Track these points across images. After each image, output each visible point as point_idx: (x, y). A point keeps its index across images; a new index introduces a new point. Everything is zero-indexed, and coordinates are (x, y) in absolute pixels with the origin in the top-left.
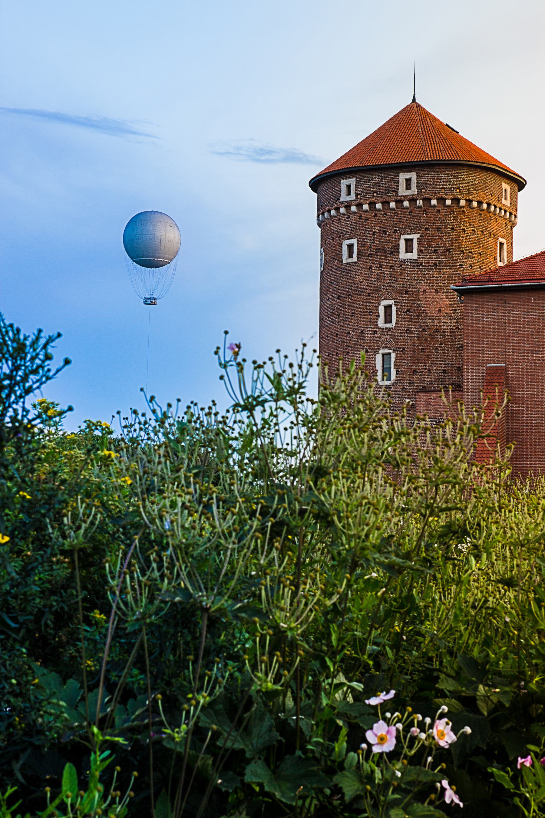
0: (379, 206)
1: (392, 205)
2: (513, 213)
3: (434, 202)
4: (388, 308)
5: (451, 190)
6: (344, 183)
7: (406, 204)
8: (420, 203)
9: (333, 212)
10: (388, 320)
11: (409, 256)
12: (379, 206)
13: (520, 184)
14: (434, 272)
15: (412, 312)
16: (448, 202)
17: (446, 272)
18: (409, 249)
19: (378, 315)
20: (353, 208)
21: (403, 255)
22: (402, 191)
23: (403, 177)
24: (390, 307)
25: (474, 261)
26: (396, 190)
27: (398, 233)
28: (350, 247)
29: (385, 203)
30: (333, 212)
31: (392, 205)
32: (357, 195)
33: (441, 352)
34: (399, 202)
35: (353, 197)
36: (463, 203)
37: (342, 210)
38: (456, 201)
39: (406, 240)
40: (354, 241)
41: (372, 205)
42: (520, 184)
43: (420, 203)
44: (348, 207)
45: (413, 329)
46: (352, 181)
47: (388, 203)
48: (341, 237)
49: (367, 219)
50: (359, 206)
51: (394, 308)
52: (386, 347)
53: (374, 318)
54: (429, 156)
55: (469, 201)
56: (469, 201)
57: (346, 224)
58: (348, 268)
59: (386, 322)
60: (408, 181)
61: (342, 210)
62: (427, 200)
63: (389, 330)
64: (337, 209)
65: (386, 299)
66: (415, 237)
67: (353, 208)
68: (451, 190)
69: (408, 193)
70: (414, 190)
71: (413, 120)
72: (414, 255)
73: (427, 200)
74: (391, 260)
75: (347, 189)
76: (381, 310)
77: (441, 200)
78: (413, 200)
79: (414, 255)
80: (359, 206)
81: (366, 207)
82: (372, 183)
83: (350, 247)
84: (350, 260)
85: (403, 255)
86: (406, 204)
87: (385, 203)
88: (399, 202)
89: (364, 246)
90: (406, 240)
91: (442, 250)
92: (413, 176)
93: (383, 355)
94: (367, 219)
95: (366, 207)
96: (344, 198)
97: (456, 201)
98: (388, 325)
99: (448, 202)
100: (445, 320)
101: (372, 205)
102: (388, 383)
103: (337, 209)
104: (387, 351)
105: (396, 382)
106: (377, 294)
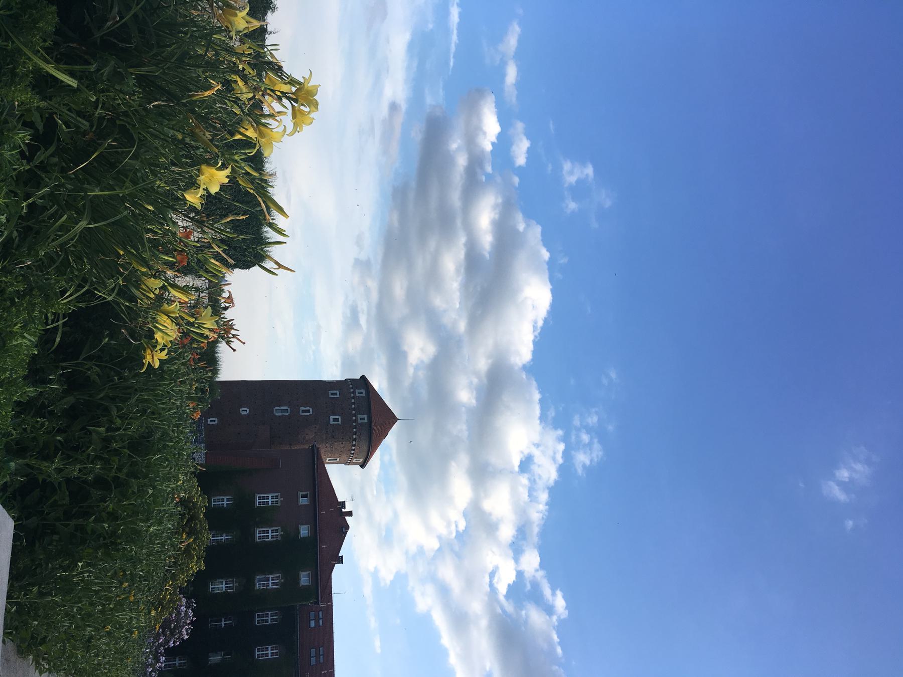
2: (349, 464)
4: (308, 411)
6: (363, 391)
10: (304, 411)
13: (363, 466)
18: (334, 420)
21: (332, 417)
22: (360, 416)
23: (365, 416)
28: (336, 394)
29: (354, 409)
41: (354, 403)
42: (363, 466)
46: (364, 395)
50: (354, 398)
54: (374, 428)
60: (364, 419)
66: (340, 422)
70: (360, 421)
71: (389, 419)
72: (332, 422)
75: (361, 392)
78: (356, 421)
79: (332, 422)
80: (354, 398)
83: (336, 394)
85: (332, 417)
88: (355, 415)
92: (366, 421)
96: (357, 391)
101: (354, 403)
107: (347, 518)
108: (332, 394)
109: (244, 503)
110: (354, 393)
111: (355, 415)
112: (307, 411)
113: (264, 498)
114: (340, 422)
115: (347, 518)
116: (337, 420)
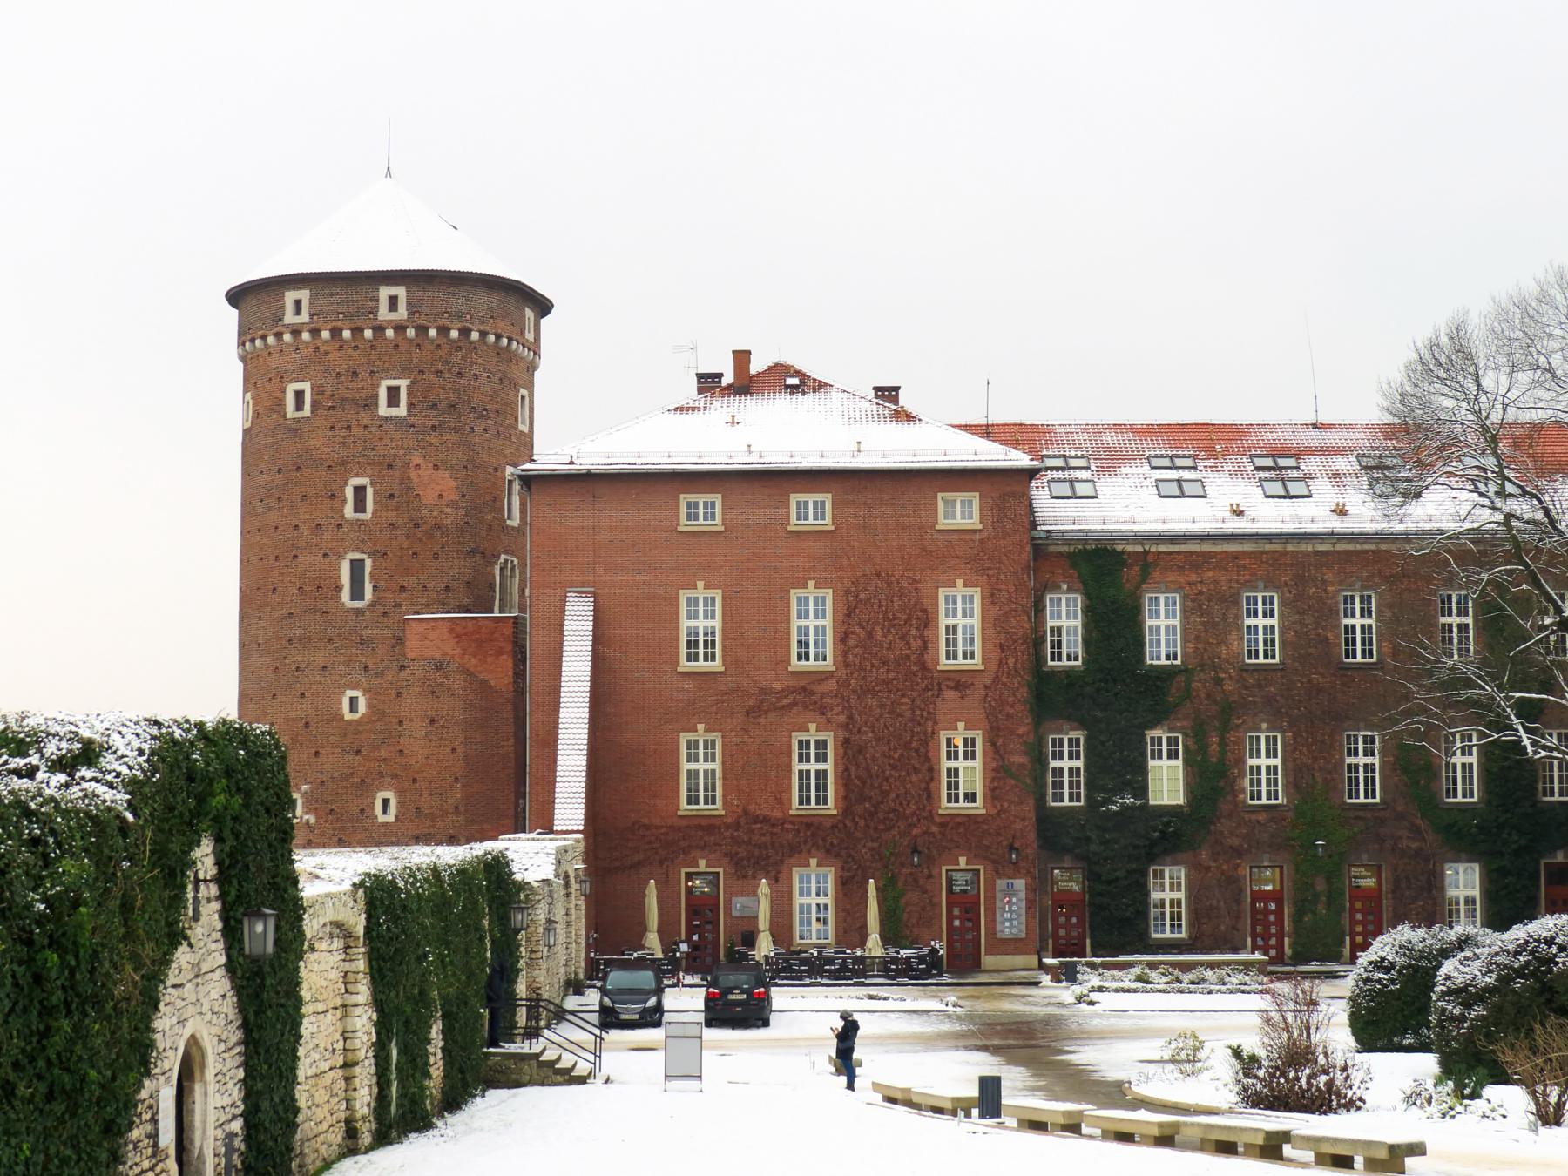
0: (347, 334)
1: (368, 333)
3: (433, 333)
4: (360, 491)
5: (459, 315)
7: (390, 333)
8: (411, 333)
9: (271, 340)
10: (360, 506)
11: (394, 412)
12: (347, 334)
14: (433, 438)
15: (398, 498)
16: (454, 334)
17: (451, 437)
19: (344, 501)
20: (306, 336)
21: (383, 410)
22: (384, 313)
23: (385, 292)
24: (363, 488)
25: (490, 422)
26: (374, 311)
27: (375, 374)
28: (299, 395)
29: (357, 331)
30: (271, 340)
31: (368, 333)
32: (312, 316)
33: (442, 558)
34: (379, 329)
35: (305, 317)
36: (475, 336)
37: (287, 337)
38: (465, 332)
39: (389, 388)
40: (306, 386)
41: (335, 332)
43: (411, 333)
44: (296, 332)
45: (400, 522)
47: (361, 330)
48: (283, 378)
49: (326, 353)
51: (370, 492)
52: (357, 549)
53: (337, 504)
55: (483, 334)
56: (483, 334)
57: (291, 361)
58: (294, 426)
59: (356, 511)
60: (393, 301)
61: (287, 337)
62: (422, 330)
63: (362, 523)
64: (279, 335)
65: (357, 475)
66: (403, 384)
67: (306, 336)
68: (459, 315)
69: (393, 316)
70: (402, 313)
72: (401, 411)
73: (422, 330)
74: (366, 418)
76: (349, 493)
77: (445, 331)
78: (400, 328)
79: (401, 411)
80: (315, 332)
81: (326, 334)
82: (337, 298)
83: (299, 395)
84: (299, 414)
85: (383, 410)
86: (390, 333)
87: (357, 331)
89: (323, 393)
90: (389, 388)
91: (443, 405)
92: (400, 291)
93: (352, 561)
94: (326, 353)
95: (326, 334)
97: (465, 332)
98: (361, 516)
99: (454, 334)
100: (449, 510)
102: (358, 604)
103: (279, 335)
104: (358, 556)
105: (373, 604)
106: (342, 468)
107: (753, 370)
108: (299, 406)
109: (710, 699)
110: (296, 332)
111: (379, 329)
112: (358, 498)
113: (692, 644)
114: (403, 384)
115: (753, 370)
116: (393, 393)
